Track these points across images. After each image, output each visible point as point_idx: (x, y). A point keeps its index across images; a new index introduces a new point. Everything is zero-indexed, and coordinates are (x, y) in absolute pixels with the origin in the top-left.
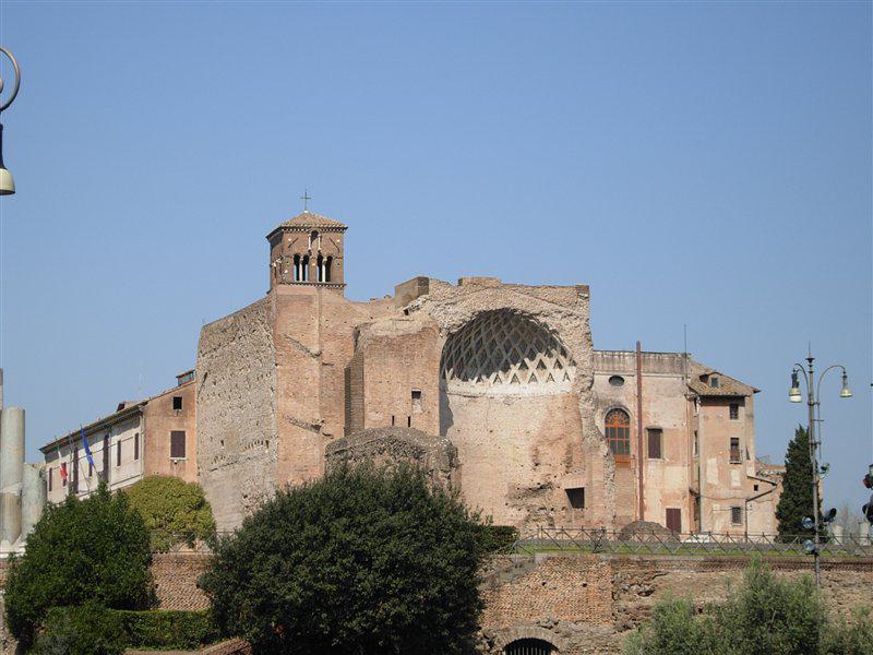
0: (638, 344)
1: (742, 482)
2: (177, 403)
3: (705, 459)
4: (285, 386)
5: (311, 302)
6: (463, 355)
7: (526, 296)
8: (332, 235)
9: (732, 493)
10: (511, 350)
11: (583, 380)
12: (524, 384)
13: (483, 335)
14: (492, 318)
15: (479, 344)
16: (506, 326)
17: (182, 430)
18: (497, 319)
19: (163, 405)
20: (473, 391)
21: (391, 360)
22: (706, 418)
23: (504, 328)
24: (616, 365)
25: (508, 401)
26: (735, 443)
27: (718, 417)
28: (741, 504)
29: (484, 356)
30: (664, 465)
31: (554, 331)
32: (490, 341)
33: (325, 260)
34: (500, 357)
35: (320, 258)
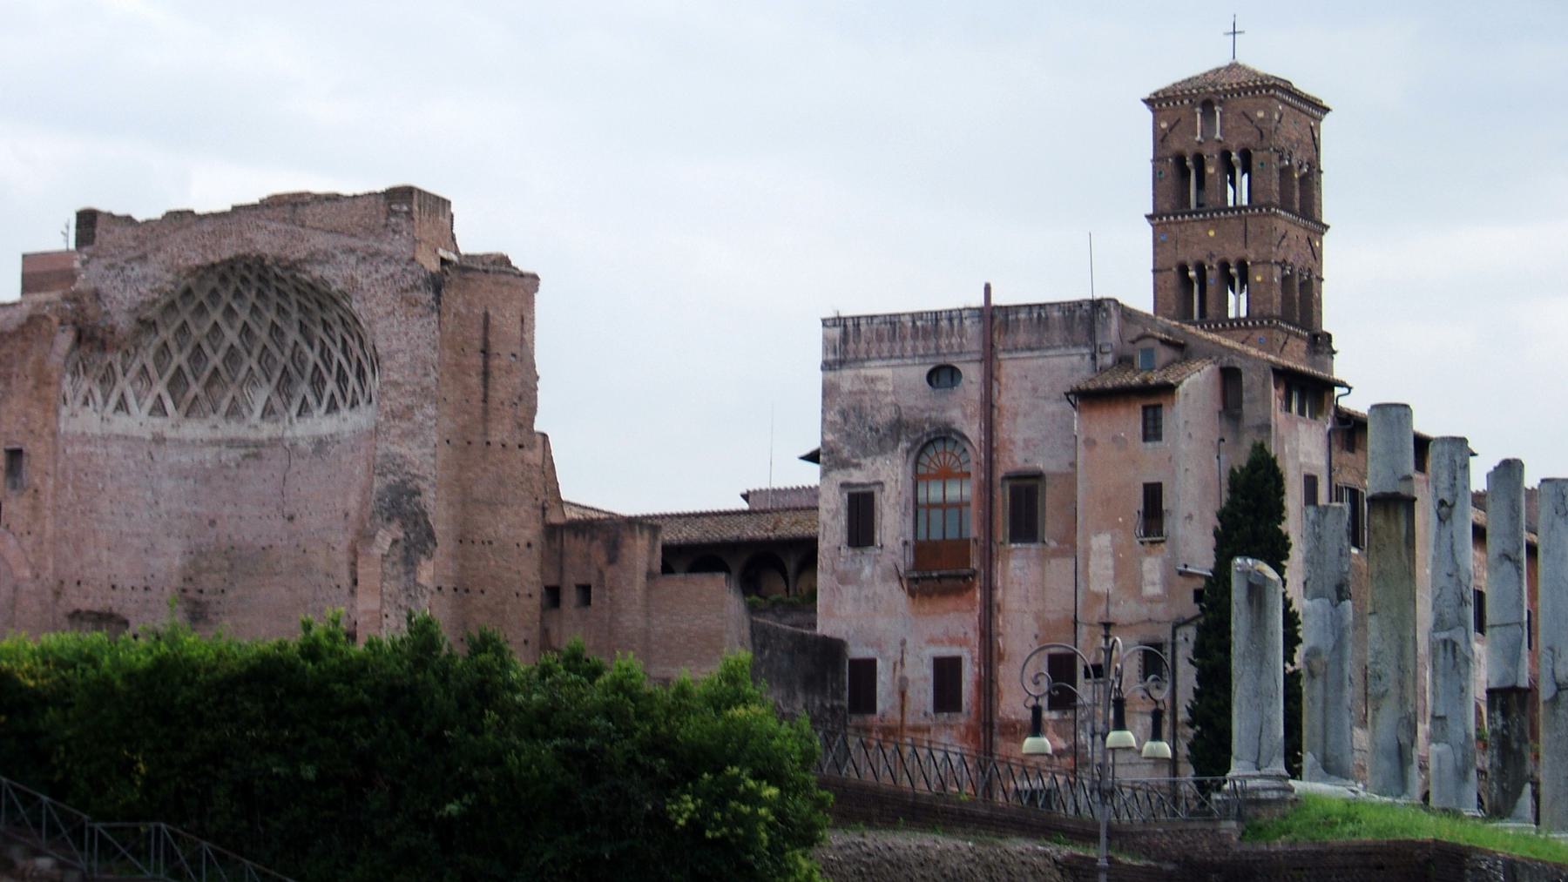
0: (988, 288)
1: (1167, 583)
3: (1086, 539)
6: (216, 360)
7: (283, 226)
8: (1246, 102)
9: (1144, 611)
10: (317, 343)
11: (393, 393)
12: (344, 411)
13: (244, 315)
14: (235, 282)
15: (246, 330)
20: (252, 435)
22: (1090, 443)
24: (943, 342)
25: (320, 444)
26: (1153, 493)
27: (1115, 439)
28: (1164, 634)
30: (1044, 558)
31: (345, 295)
32: (266, 330)
33: (1235, 157)
34: (297, 357)
35: (1226, 155)
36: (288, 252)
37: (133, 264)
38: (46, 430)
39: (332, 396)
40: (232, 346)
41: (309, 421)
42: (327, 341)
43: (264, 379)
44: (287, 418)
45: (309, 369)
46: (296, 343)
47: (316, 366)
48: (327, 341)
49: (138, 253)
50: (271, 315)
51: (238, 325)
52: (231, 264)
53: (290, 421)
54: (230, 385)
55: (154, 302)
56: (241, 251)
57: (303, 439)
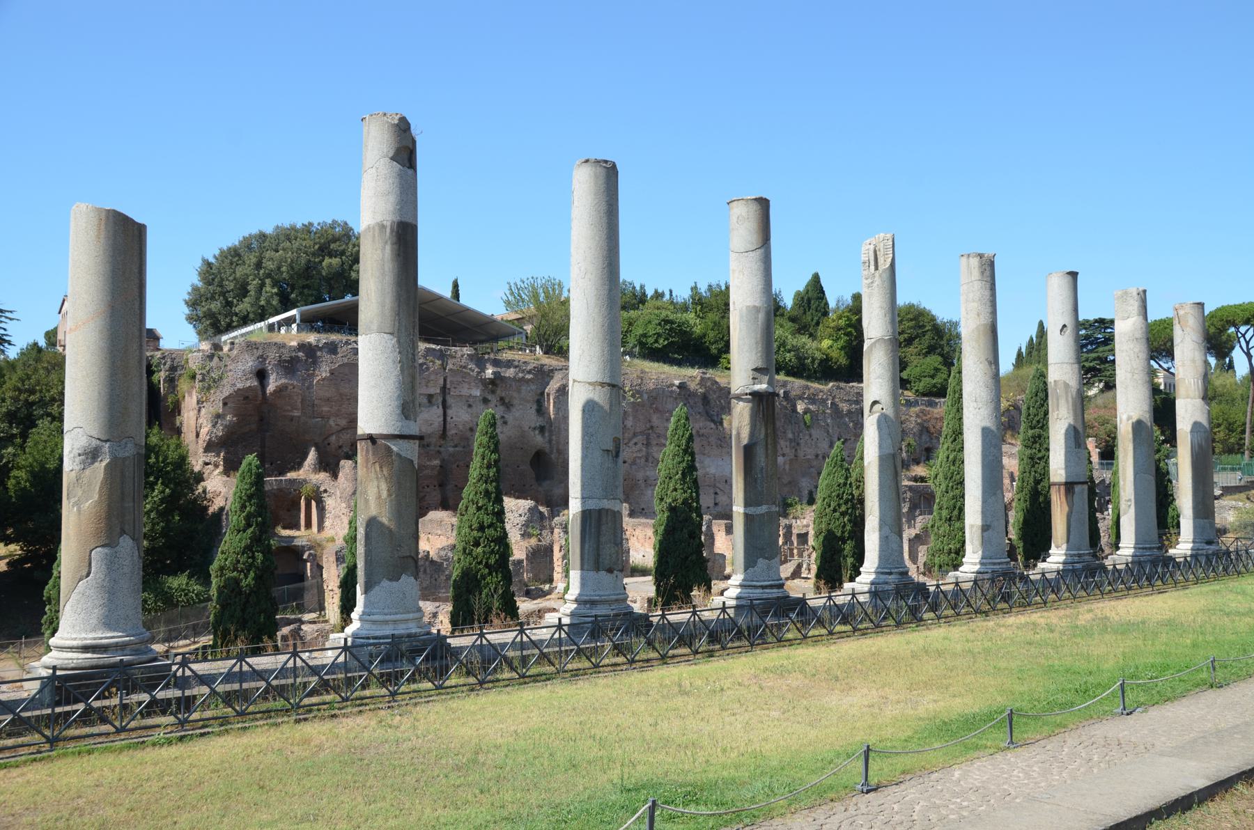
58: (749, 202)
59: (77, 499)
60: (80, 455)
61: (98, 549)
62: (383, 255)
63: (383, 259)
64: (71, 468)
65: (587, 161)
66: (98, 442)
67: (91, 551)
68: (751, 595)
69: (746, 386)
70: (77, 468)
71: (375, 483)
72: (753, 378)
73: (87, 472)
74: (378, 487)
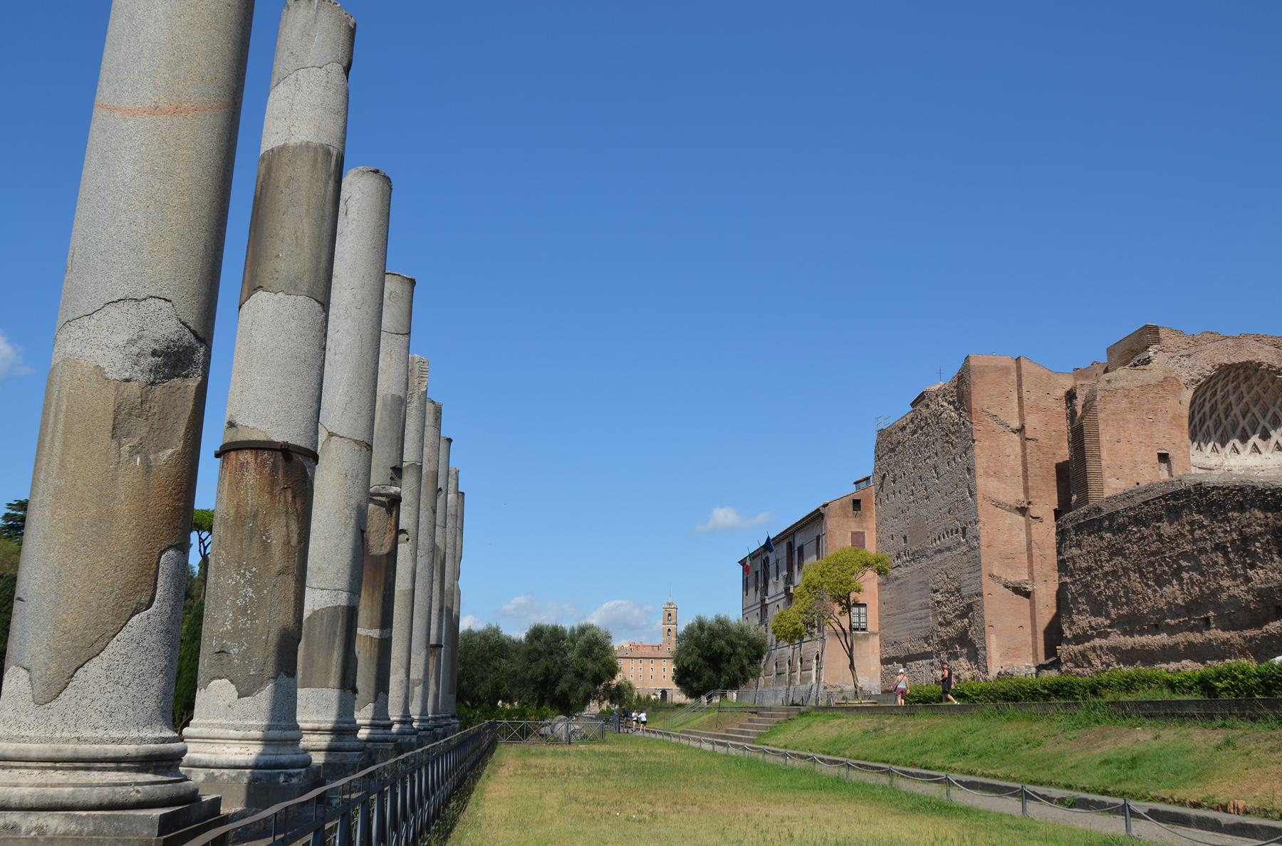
2: (857, 504)
4: (985, 465)
5: (1008, 373)
7: (1273, 349)
10: (1249, 415)
12: (1266, 454)
13: (1219, 395)
14: (1232, 374)
16: (1246, 385)
17: (861, 530)
18: (1237, 377)
19: (842, 507)
21: (1130, 417)
23: (1243, 387)
29: (1218, 424)
32: (1225, 405)
36: (1276, 363)
37: (1185, 358)
38: (1183, 443)
39: (1255, 444)
40: (1204, 413)
41: (1238, 457)
42: (1258, 415)
43: (1213, 433)
44: (1224, 454)
45: (1239, 429)
46: (1235, 415)
47: (1243, 428)
48: (1258, 415)
49: (1186, 352)
50: (1232, 398)
51: (1213, 401)
52: (1242, 364)
53: (1225, 457)
54: (1198, 434)
55: (1199, 380)
56: (1250, 359)
57: (1235, 466)
58: (405, 281)
59: (136, 441)
60: (154, 353)
61: (171, 552)
62: (326, 191)
63: (324, 197)
64: (127, 375)
65: (376, 172)
66: (193, 340)
67: (162, 552)
68: (376, 736)
69: (384, 485)
70: (143, 378)
71: (283, 521)
72: (392, 478)
73: (158, 391)
74: (287, 528)
